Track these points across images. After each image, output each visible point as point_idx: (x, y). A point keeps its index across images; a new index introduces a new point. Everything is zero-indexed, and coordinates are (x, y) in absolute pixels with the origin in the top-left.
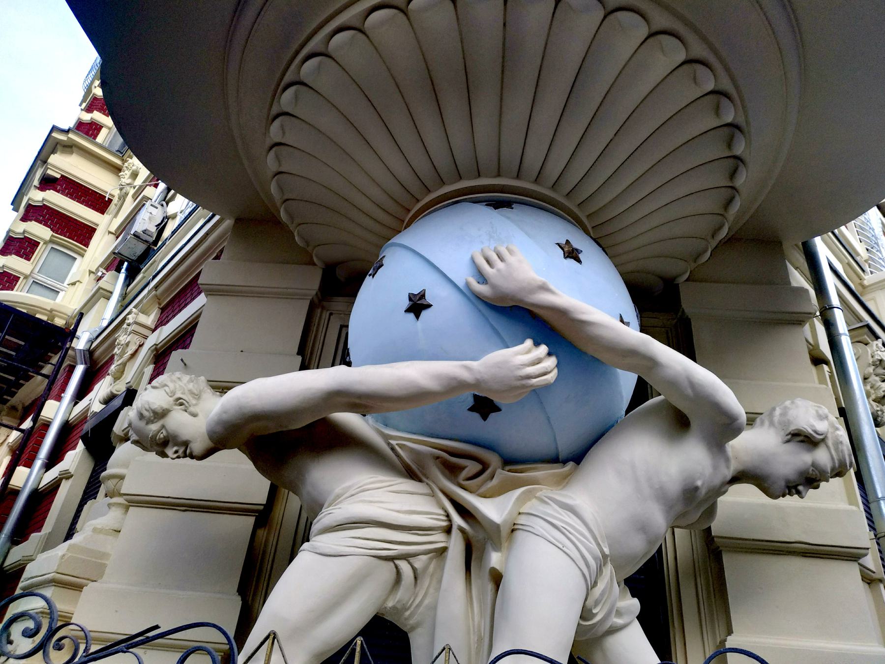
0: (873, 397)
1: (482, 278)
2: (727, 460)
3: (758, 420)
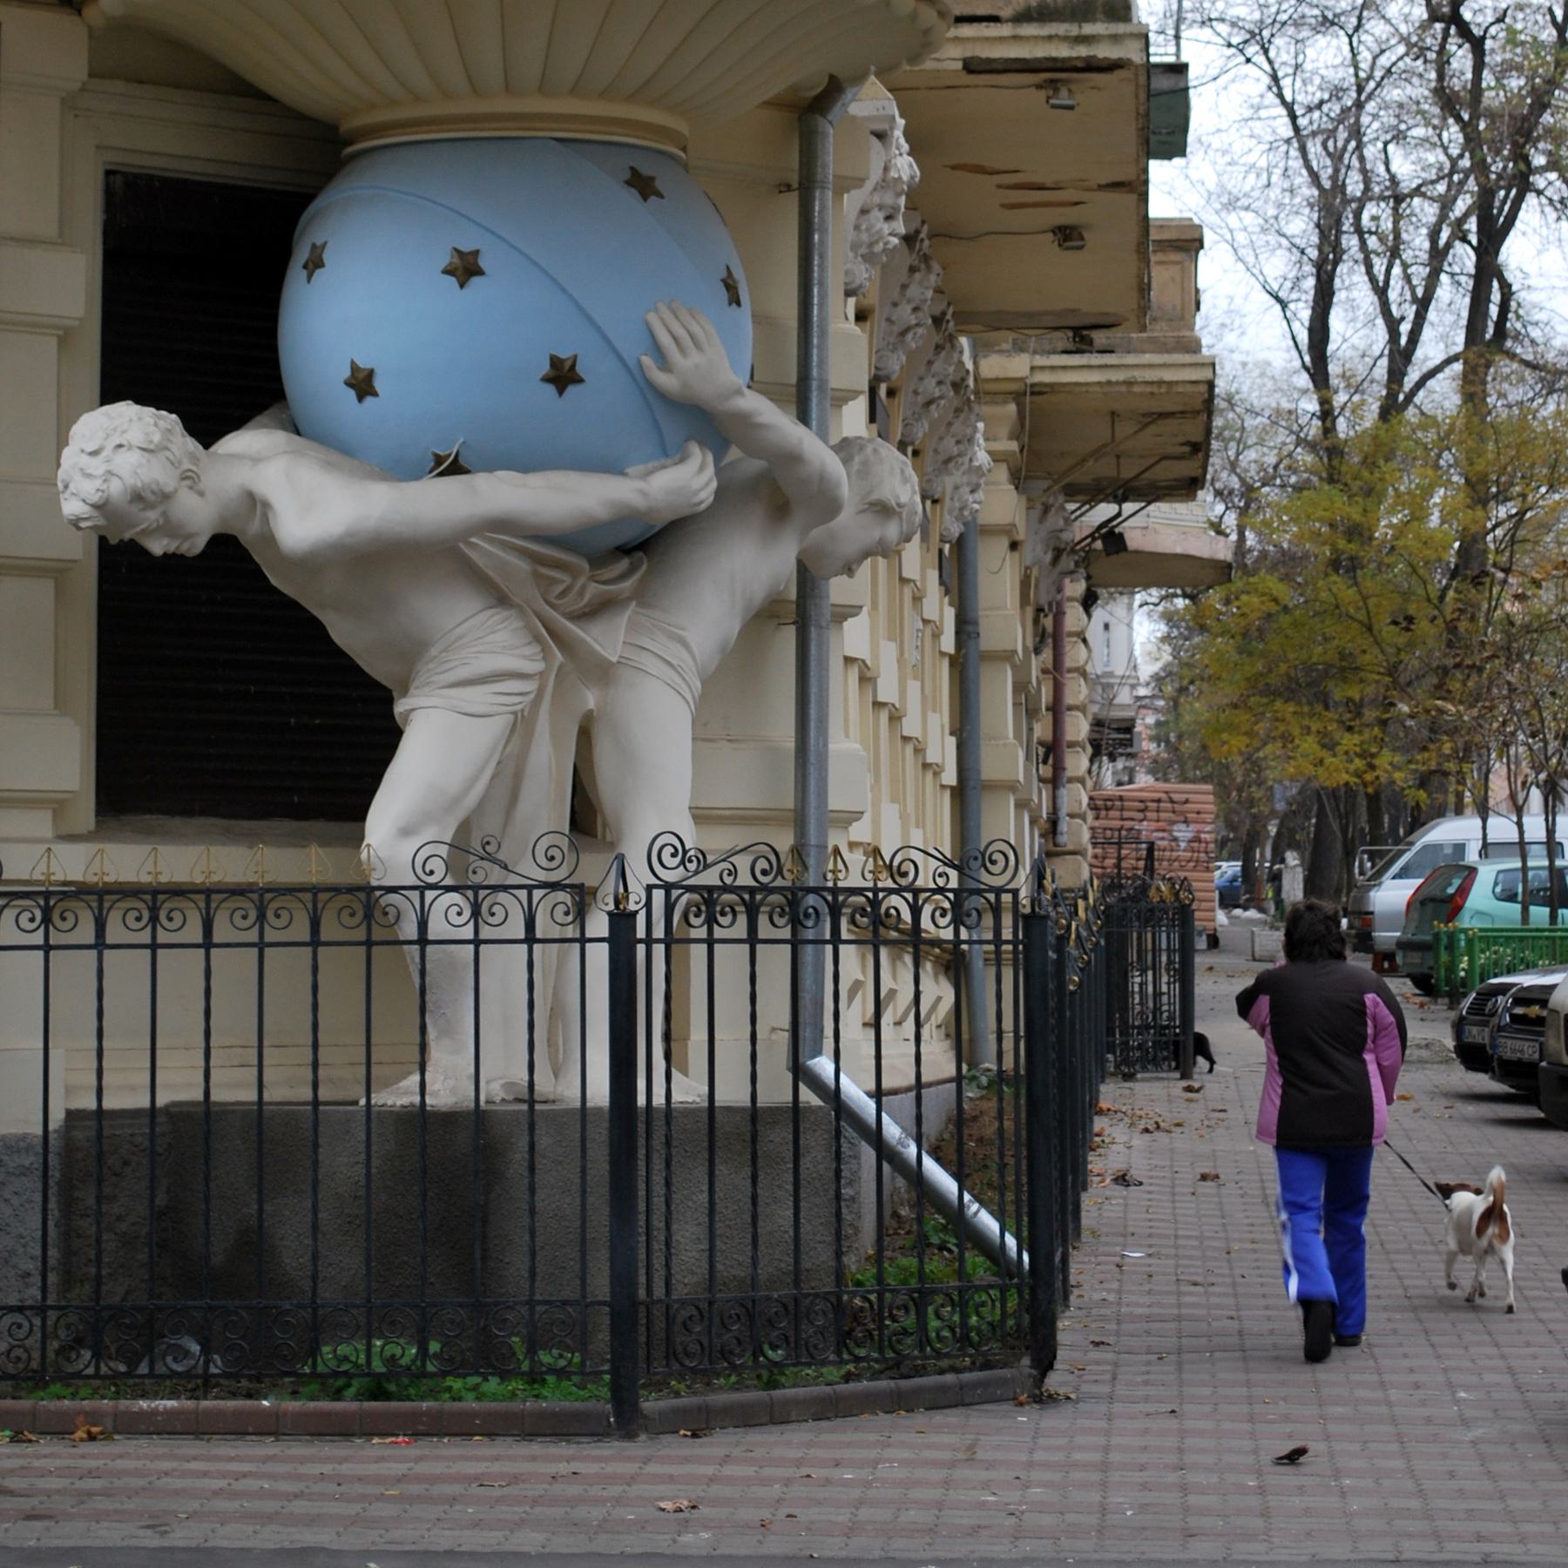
0: (863, 250)
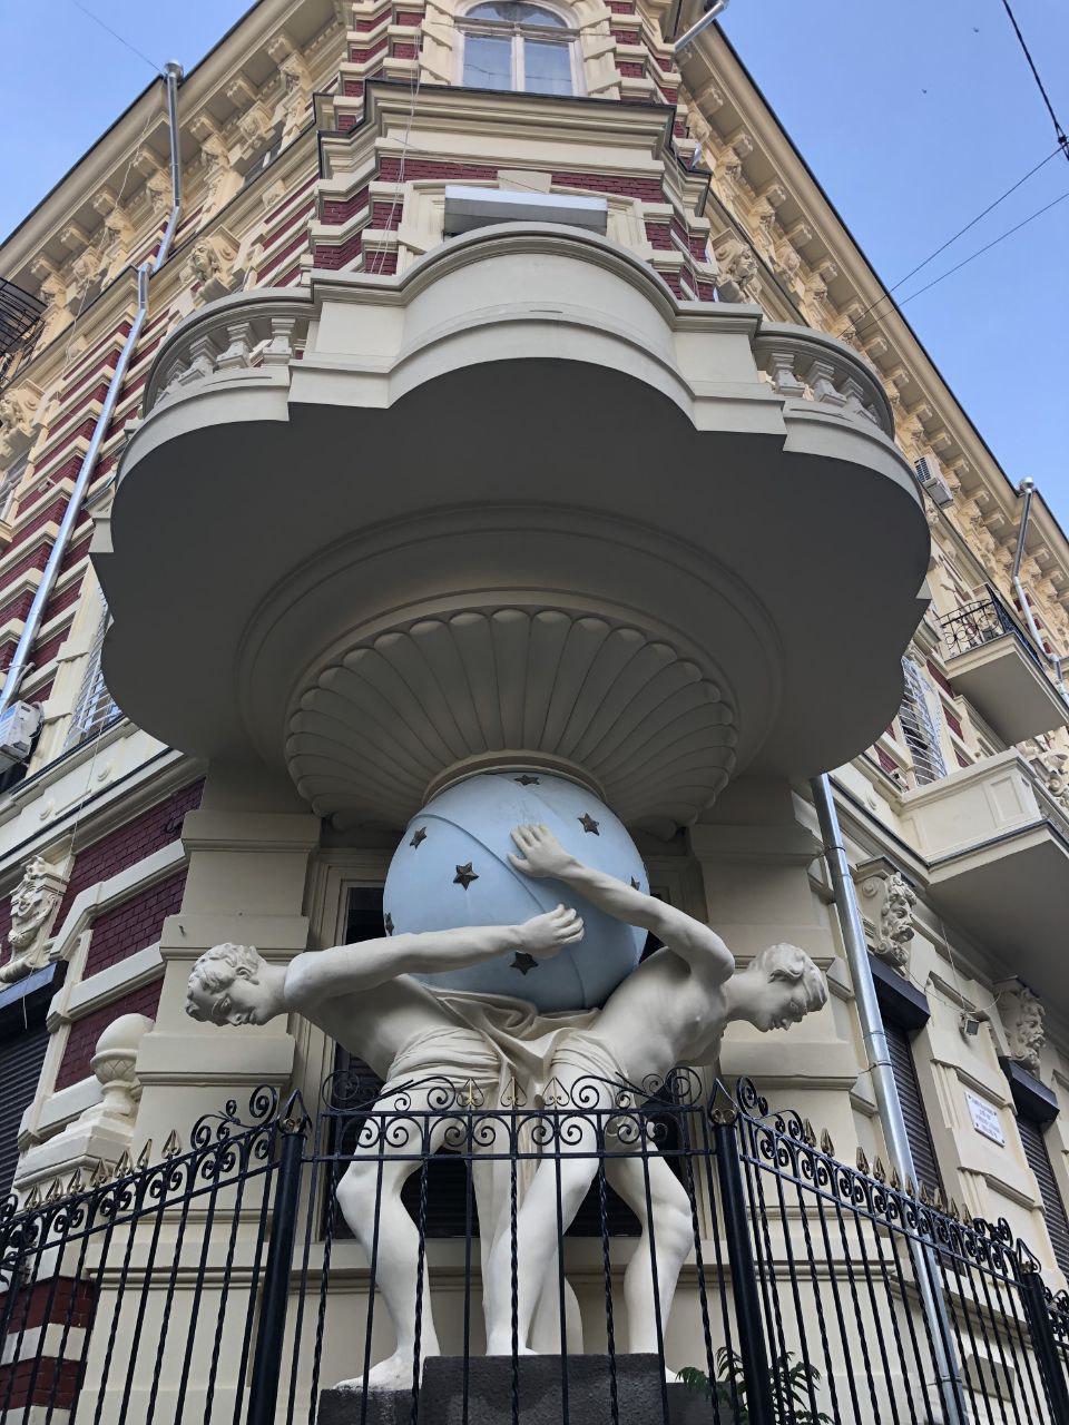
0: (891, 934)
1: (524, 856)
2: (723, 999)
3: (751, 964)
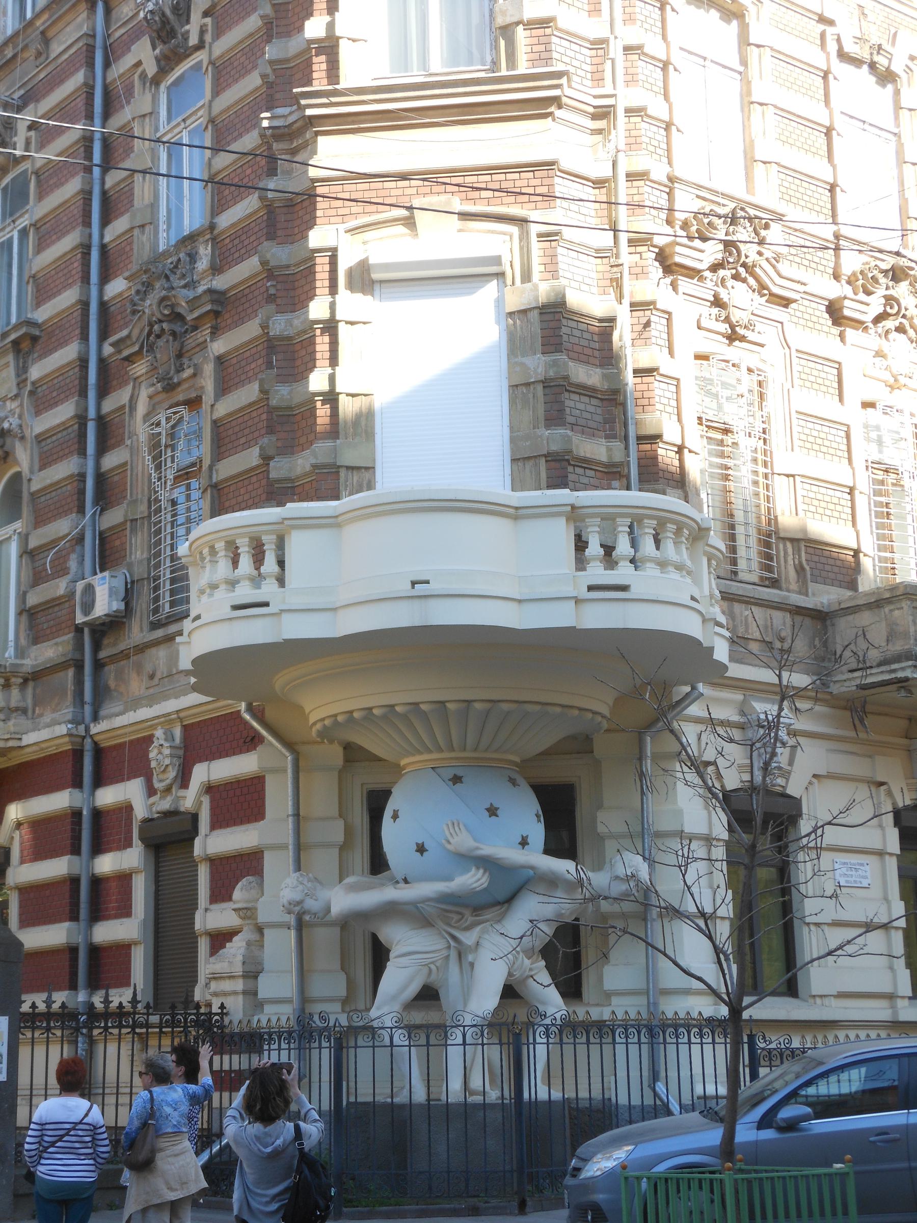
1: (449, 842)
